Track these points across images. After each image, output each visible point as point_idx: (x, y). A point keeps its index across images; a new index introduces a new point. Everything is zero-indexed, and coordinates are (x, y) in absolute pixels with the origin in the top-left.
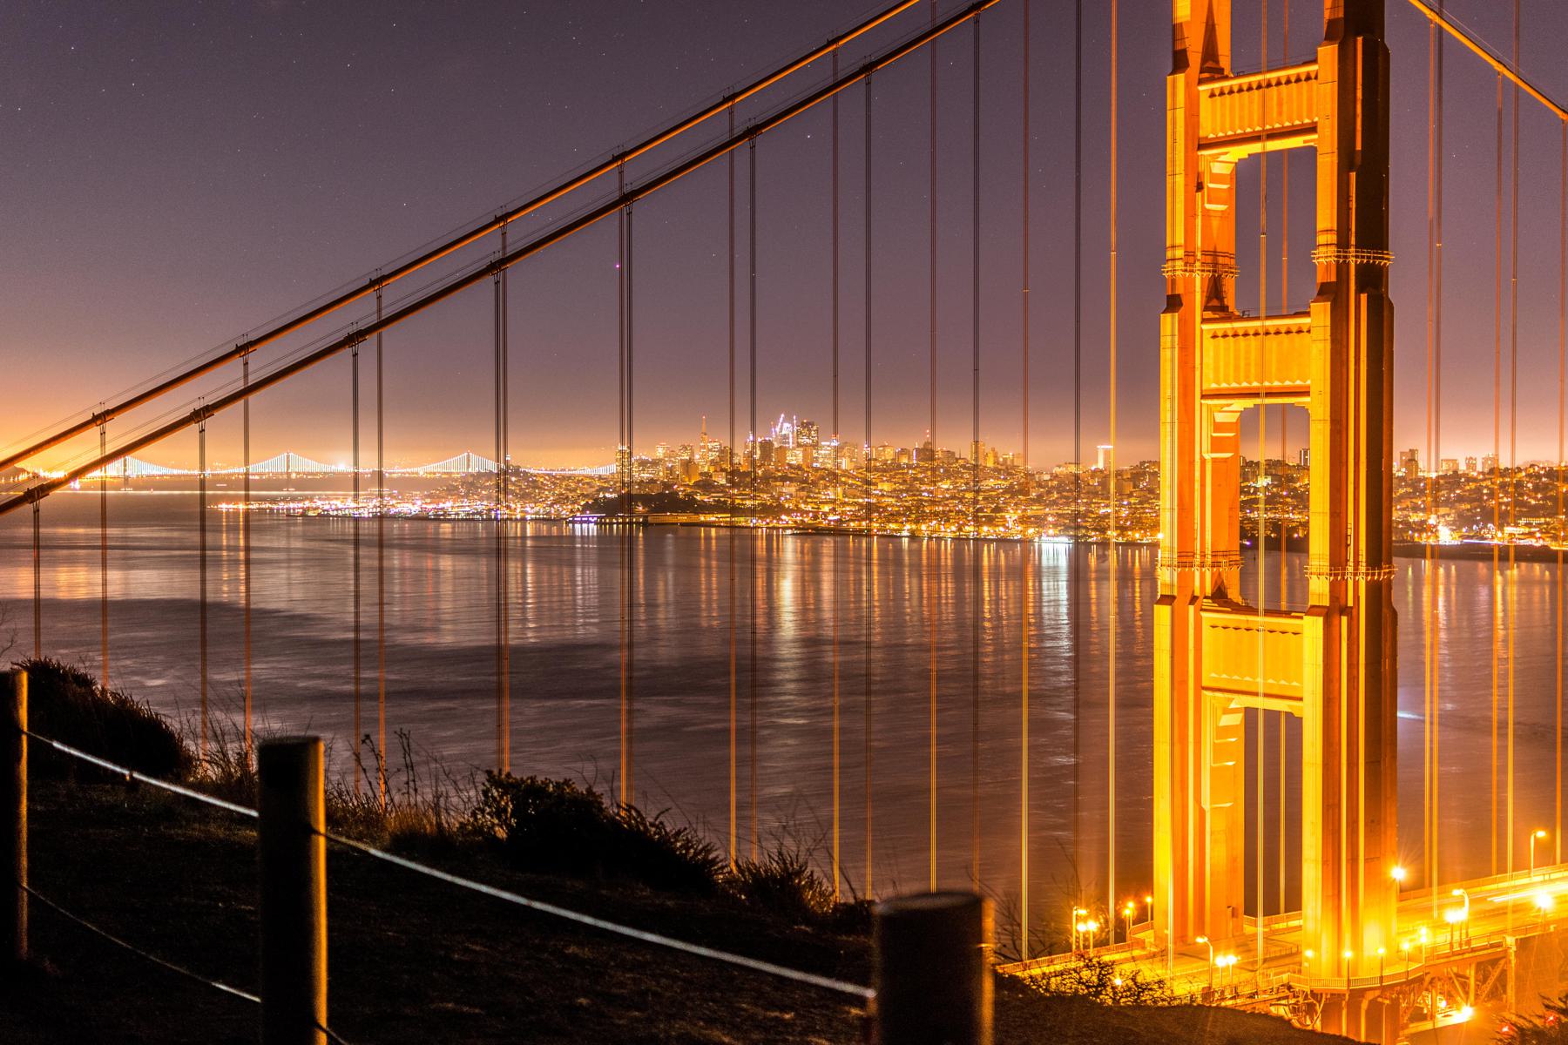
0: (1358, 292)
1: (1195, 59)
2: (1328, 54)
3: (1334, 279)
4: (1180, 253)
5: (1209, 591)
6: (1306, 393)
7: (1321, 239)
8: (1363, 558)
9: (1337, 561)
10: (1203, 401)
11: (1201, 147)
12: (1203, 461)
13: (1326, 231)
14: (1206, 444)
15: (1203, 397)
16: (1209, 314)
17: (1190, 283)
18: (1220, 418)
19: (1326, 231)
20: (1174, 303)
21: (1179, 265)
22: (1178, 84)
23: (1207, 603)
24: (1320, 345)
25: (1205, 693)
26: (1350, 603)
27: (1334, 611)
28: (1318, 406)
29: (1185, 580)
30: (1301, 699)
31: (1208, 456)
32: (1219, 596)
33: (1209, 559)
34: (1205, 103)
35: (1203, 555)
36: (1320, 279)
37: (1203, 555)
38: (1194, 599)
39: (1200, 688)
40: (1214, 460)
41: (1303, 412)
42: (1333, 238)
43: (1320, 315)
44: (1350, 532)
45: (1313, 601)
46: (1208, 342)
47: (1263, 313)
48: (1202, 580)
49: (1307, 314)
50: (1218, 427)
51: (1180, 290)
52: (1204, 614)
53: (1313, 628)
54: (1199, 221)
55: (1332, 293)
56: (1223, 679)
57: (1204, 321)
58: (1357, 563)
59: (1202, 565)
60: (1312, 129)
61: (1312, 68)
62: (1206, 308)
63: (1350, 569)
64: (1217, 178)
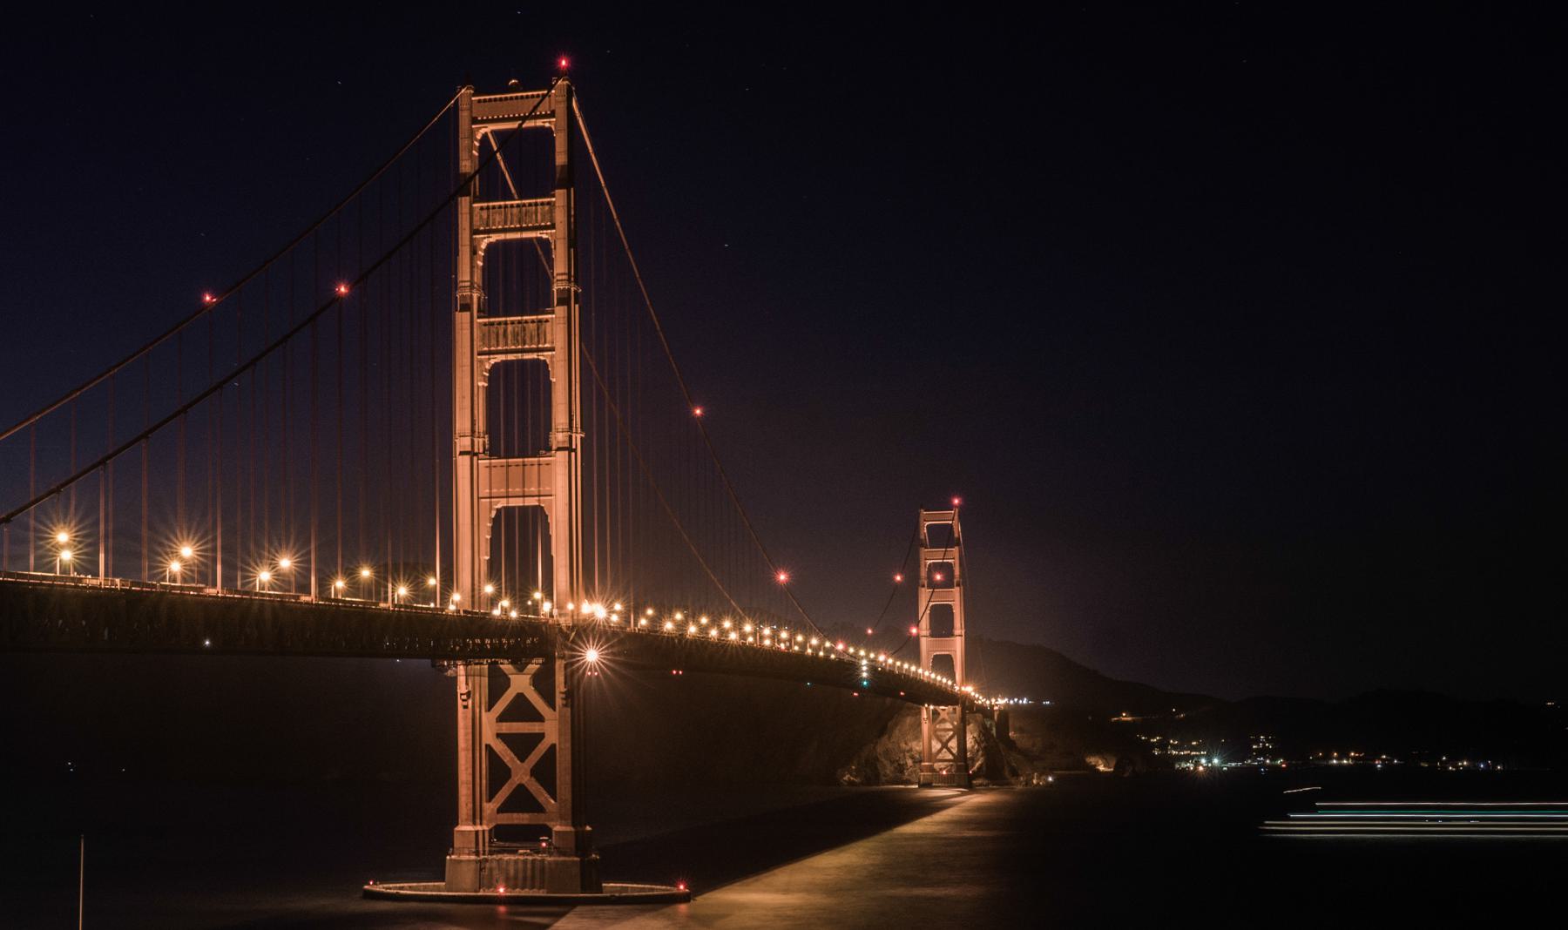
0: (575, 303)
5: (481, 451)
6: (552, 349)
8: (579, 426)
10: (479, 357)
11: (475, 234)
12: (478, 387)
13: (562, 274)
15: (479, 354)
16: (482, 314)
17: (471, 297)
19: (562, 274)
20: (467, 307)
22: (464, 202)
24: (562, 326)
26: (574, 447)
30: (551, 495)
33: (482, 435)
34: (476, 212)
38: (476, 454)
39: (478, 498)
42: (565, 277)
45: (561, 446)
48: (480, 443)
49: (553, 312)
51: (469, 301)
52: (480, 462)
54: (476, 270)
57: (479, 317)
59: (479, 437)
62: (479, 311)
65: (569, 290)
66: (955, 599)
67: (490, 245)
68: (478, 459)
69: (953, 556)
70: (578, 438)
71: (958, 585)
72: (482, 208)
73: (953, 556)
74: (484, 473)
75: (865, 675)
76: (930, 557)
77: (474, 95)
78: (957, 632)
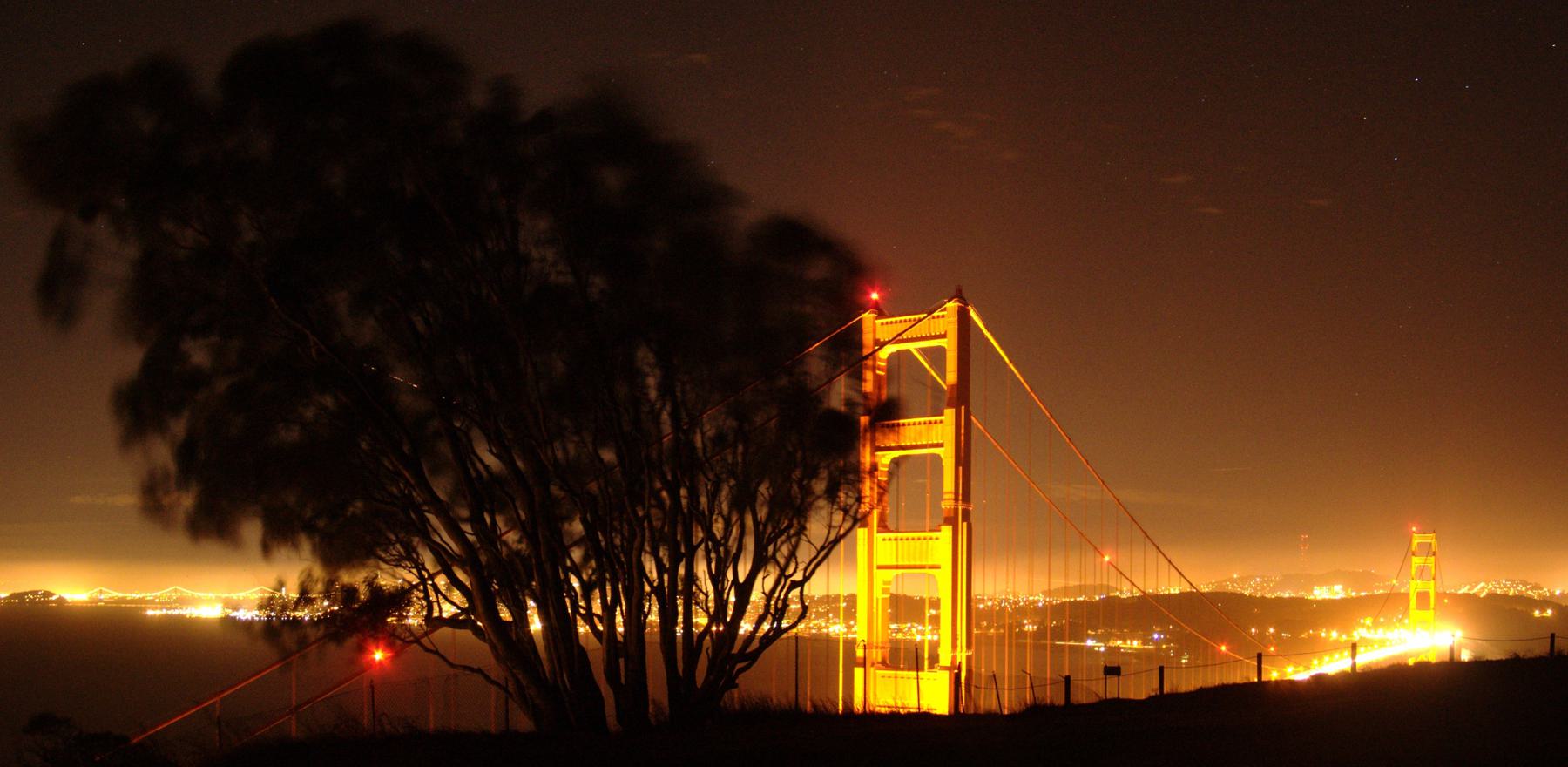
0: (963, 521)
2: (949, 414)
3: (952, 515)
6: (937, 567)
7: (946, 496)
9: (954, 646)
15: (880, 567)
16: (880, 529)
28: (944, 577)
32: (885, 664)
36: (945, 515)
42: (952, 496)
43: (947, 531)
44: (959, 632)
46: (880, 542)
47: (927, 529)
52: (880, 672)
55: (951, 521)
62: (879, 526)
63: (959, 648)
64: (884, 466)
65: (956, 510)
71: (1434, 579)
76: (1417, 561)
77: (877, 318)
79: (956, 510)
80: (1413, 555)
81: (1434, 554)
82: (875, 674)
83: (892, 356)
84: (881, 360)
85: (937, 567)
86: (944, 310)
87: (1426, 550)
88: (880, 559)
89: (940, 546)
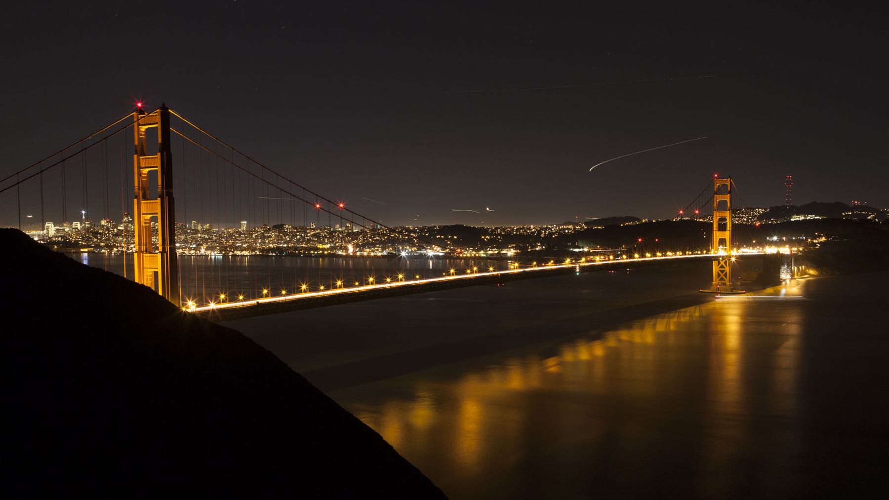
1: (139, 153)
2: (159, 154)
3: (161, 193)
4: (137, 188)
6: (157, 214)
7: (159, 187)
8: (168, 243)
12: (143, 226)
14: (143, 223)
15: (143, 214)
18: (146, 218)
20: (136, 197)
21: (137, 190)
22: (135, 156)
23: (144, 252)
25: (145, 269)
27: (162, 253)
28: (159, 216)
29: (140, 248)
31: (144, 225)
34: (141, 160)
35: (143, 243)
37: (143, 243)
38: (142, 252)
39: (143, 268)
40: (145, 226)
41: (157, 217)
43: (159, 200)
48: (143, 248)
50: (145, 220)
51: (137, 194)
53: (159, 255)
56: (148, 266)
58: (167, 244)
60: (157, 167)
61: (157, 156)
66: (727, 215)
67: (149, 171)
68: (143, 253)
69: (727, 198)
70: (168, 248)
71: (729, 210)
72: (142, 159)
73: (727, 198)
74: (144, 257)
75: (578, 270)
76: (718, 198)
77: (139, 115)
78: (728, 229)
79: (163, 192)
80: (716, 193)
81: (730, 192)
82: (143, 256)
83: (147, 129)
84: (141, 132)
85: (157, 214)
86: (157, 112)
87: (722, 190)
88: (143, 211)
89: (156, 206)
